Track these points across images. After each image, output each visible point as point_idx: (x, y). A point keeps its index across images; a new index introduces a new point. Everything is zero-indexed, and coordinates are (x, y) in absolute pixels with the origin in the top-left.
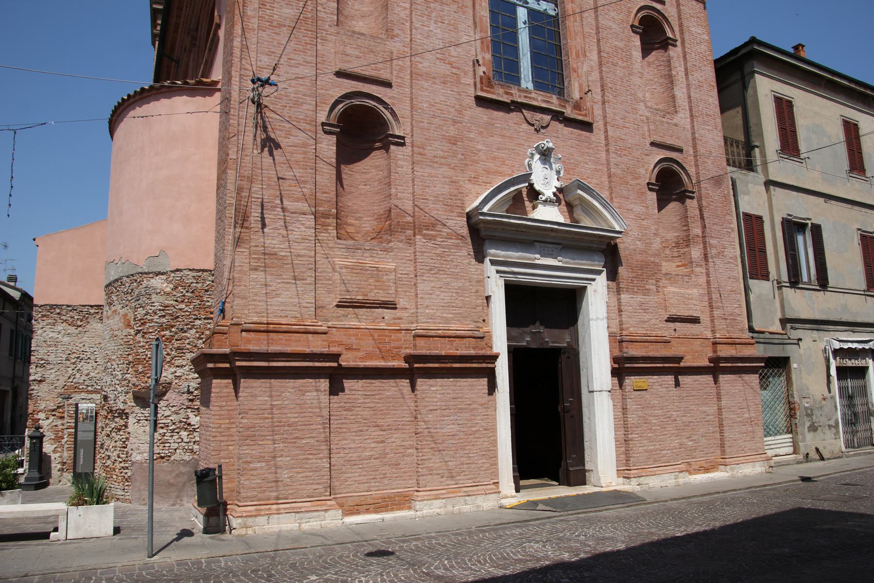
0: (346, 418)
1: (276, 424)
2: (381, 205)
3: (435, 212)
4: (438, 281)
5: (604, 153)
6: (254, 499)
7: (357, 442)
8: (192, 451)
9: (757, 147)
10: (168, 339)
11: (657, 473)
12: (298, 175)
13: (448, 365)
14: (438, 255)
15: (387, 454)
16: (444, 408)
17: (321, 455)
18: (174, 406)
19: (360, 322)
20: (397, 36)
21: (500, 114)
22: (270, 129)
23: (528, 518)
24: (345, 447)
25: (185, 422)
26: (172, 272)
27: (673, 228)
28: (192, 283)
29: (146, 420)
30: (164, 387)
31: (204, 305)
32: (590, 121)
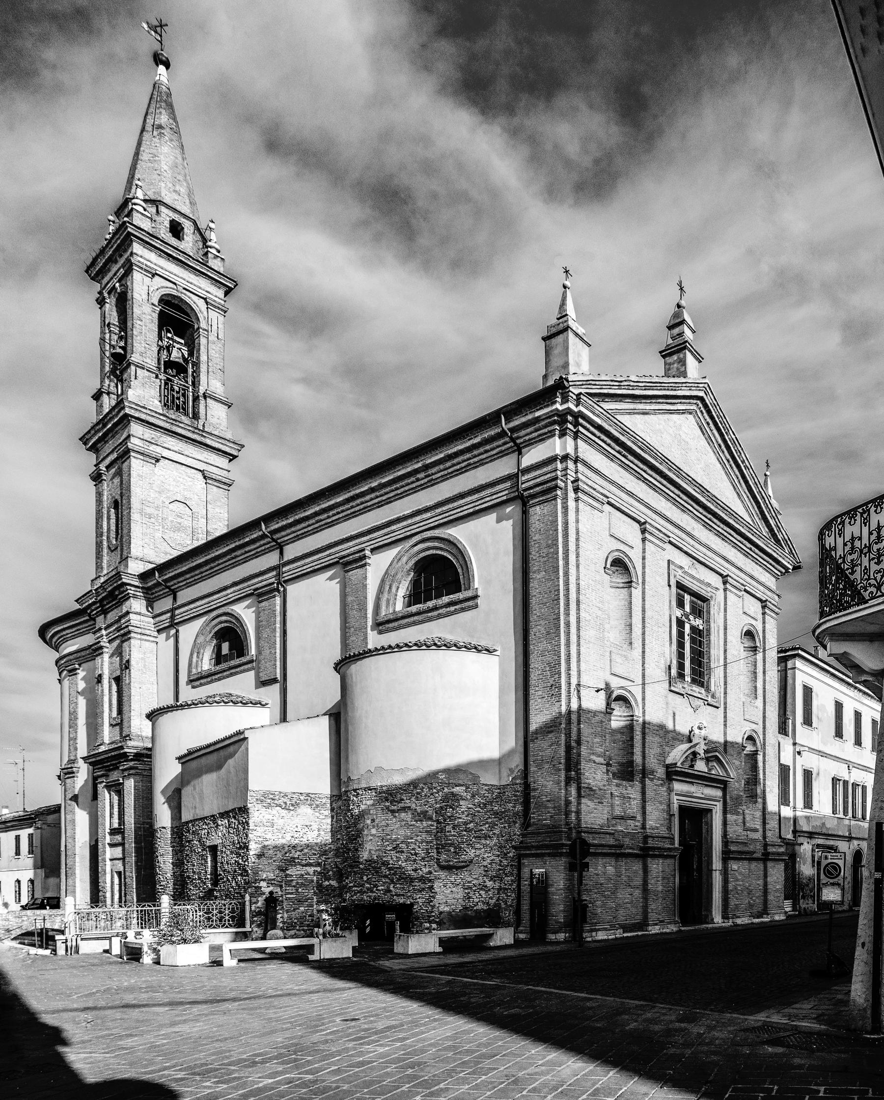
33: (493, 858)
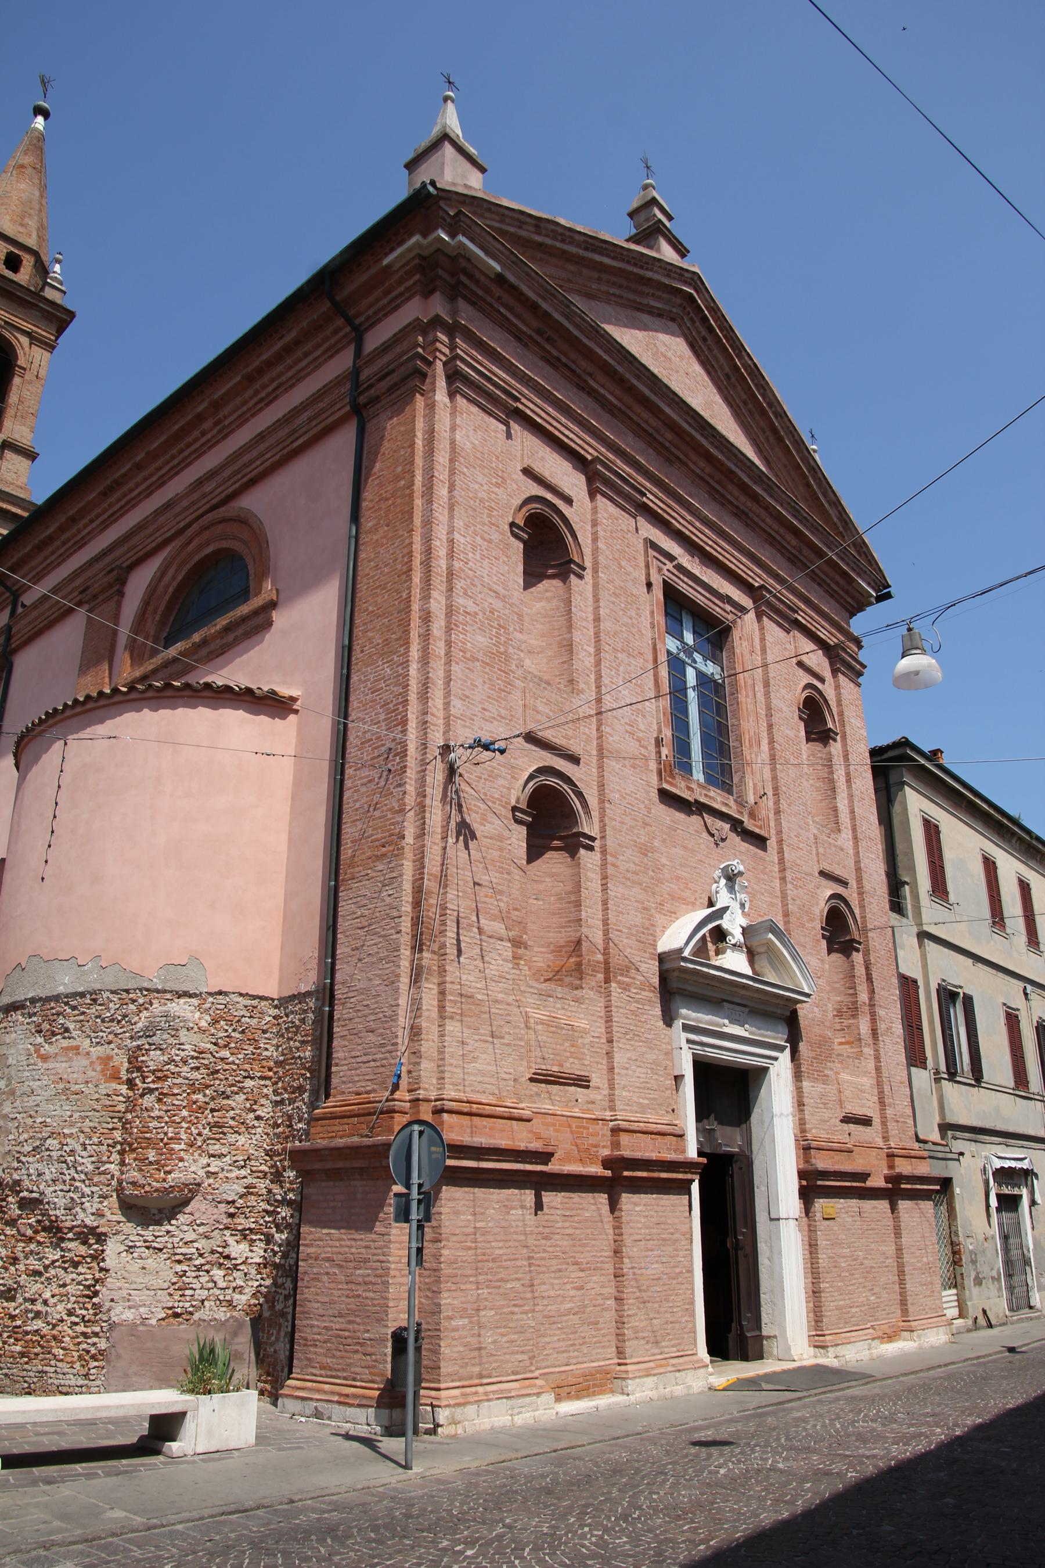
0: (545, 1251)
1: (480, 1258)
2: (560, 932)
3: (629, 950)
4: (634, 1050)
5: (778, 881)
6: (455, 1377)
7: (556, 1287)
8: (230, 1303)
9: (908, 884)
10: (200, 1108)
11: (852, 1340)
12: (494, 880)
13: (656, 1175)
14: (633, 1013)
15: (585, 1307)
16: (648, 1237)
17: (526, 1308)
18: (203, 1224)
19: (553, 1105)
20: (582, 691)
21: (680, 816)
22: (465, 809)
23: (780, 1400)
24: (544, 1294)
25: (221, 1253)
26: (210, 994)
27: (834, 989)
28: (243, 1016)
29: (148, 1248)
30: (190, 1190)
31: (260, 1054)
32: (766, 835)
33: (250, 1180)
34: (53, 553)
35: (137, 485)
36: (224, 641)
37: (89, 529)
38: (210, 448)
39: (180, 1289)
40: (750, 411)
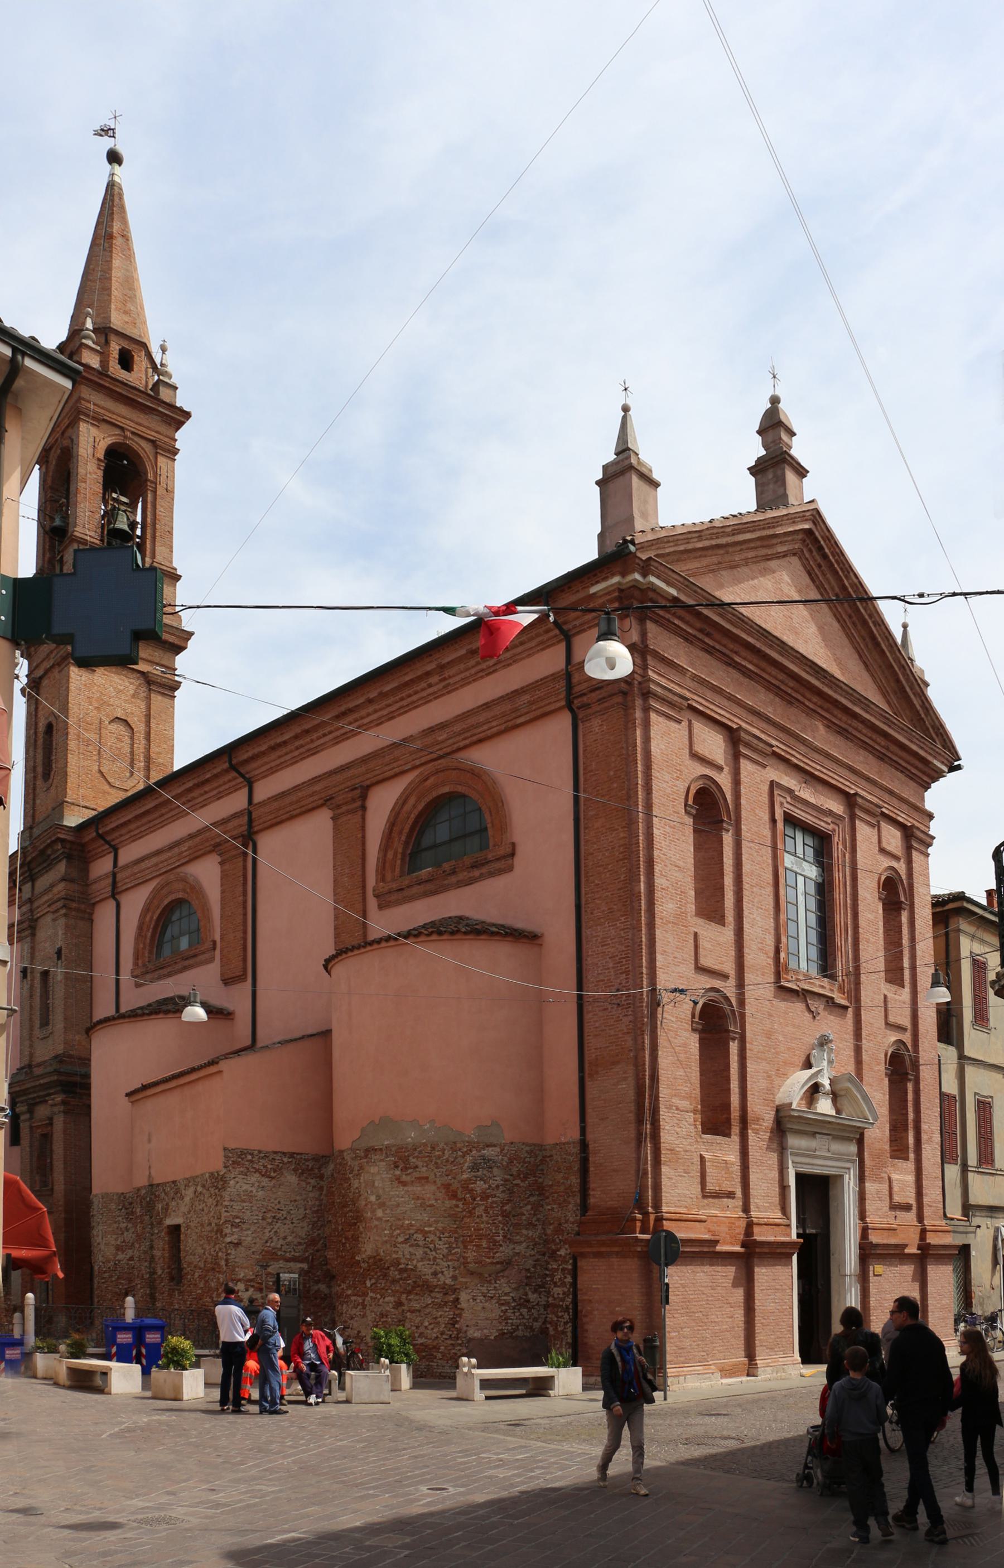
0: (712, 1296)
8: (531, 1327)
34: (287, 754)
35: (369, 715)
36: (471, 875)
37: (322, 741)
38: (436, 698)
39: (505, 1319)
40: (854, 624)
